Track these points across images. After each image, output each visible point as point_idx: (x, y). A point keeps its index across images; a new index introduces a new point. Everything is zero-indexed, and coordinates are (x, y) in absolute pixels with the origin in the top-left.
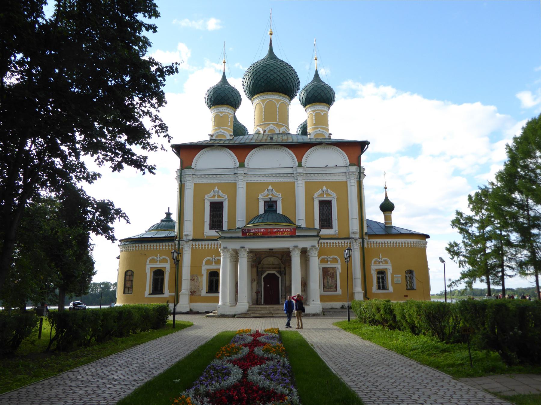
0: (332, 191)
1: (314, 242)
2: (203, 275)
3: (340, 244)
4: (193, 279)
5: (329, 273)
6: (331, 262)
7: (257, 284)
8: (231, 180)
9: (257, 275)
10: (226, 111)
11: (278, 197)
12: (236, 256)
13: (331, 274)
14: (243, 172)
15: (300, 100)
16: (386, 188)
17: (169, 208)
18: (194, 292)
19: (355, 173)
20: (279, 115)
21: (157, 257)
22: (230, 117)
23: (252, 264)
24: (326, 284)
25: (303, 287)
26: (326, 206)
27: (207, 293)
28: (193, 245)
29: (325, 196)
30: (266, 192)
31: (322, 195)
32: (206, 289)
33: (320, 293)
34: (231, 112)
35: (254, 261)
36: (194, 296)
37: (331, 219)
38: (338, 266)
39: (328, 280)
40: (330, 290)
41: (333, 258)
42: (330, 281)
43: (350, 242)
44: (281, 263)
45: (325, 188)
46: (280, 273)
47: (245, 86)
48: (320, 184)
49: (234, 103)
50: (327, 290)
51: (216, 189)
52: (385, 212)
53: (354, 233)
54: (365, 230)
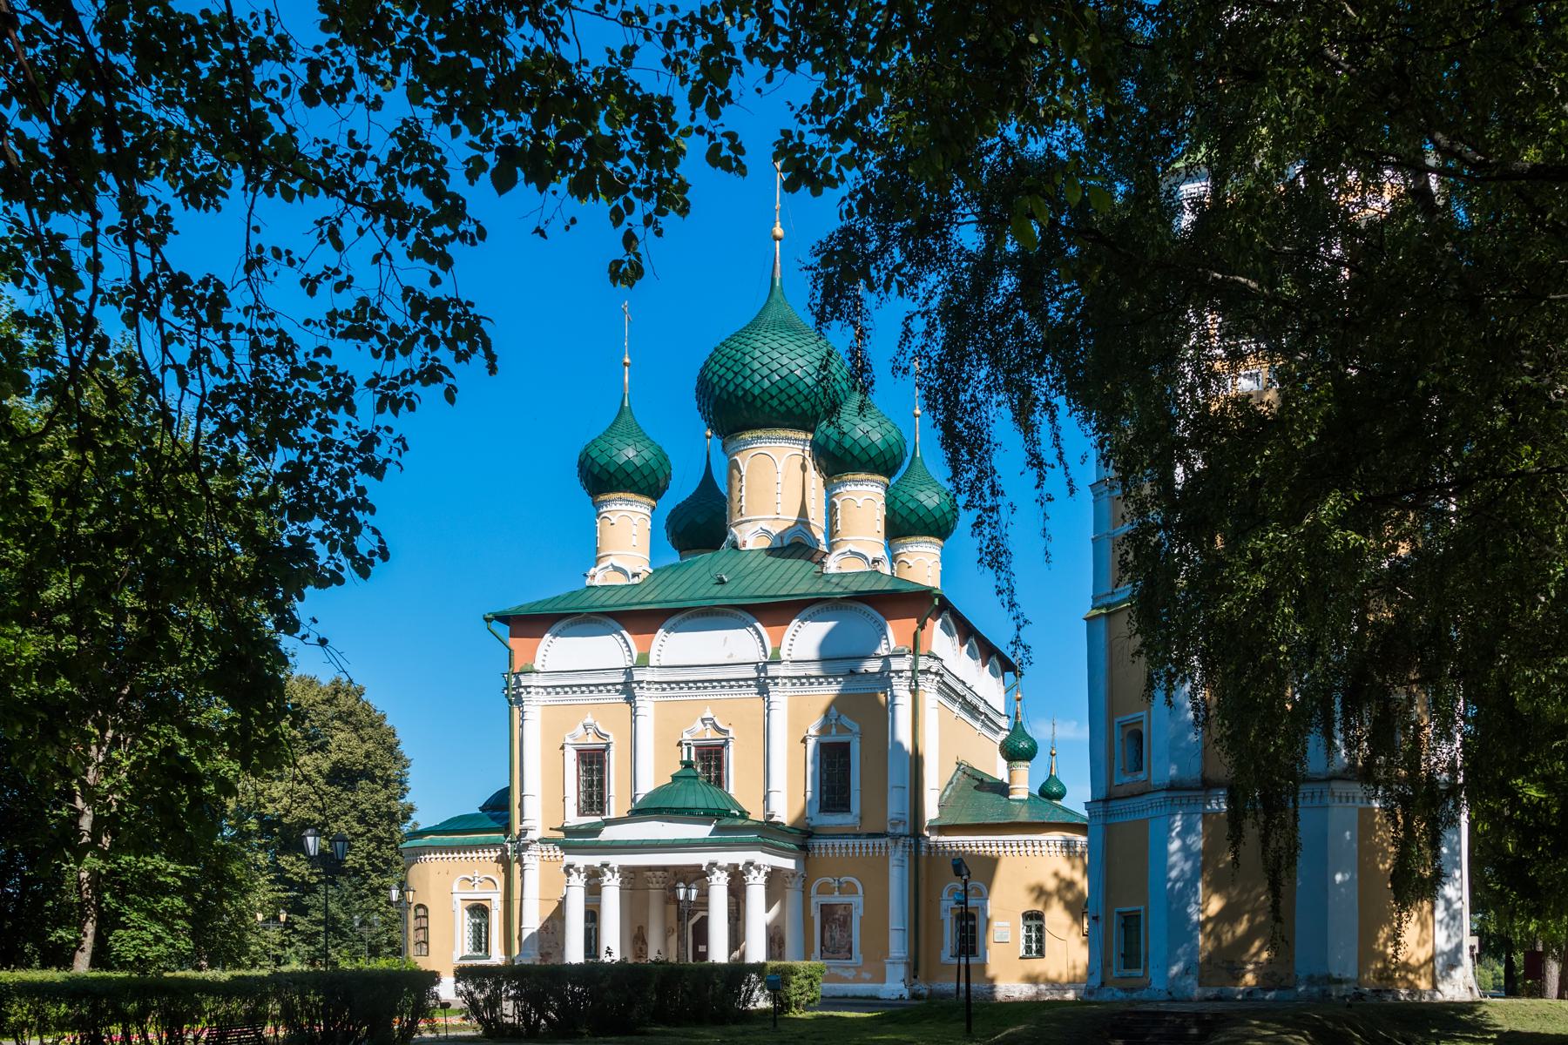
38: (857, 901)
42: (837, 936)
50: (830, 955)
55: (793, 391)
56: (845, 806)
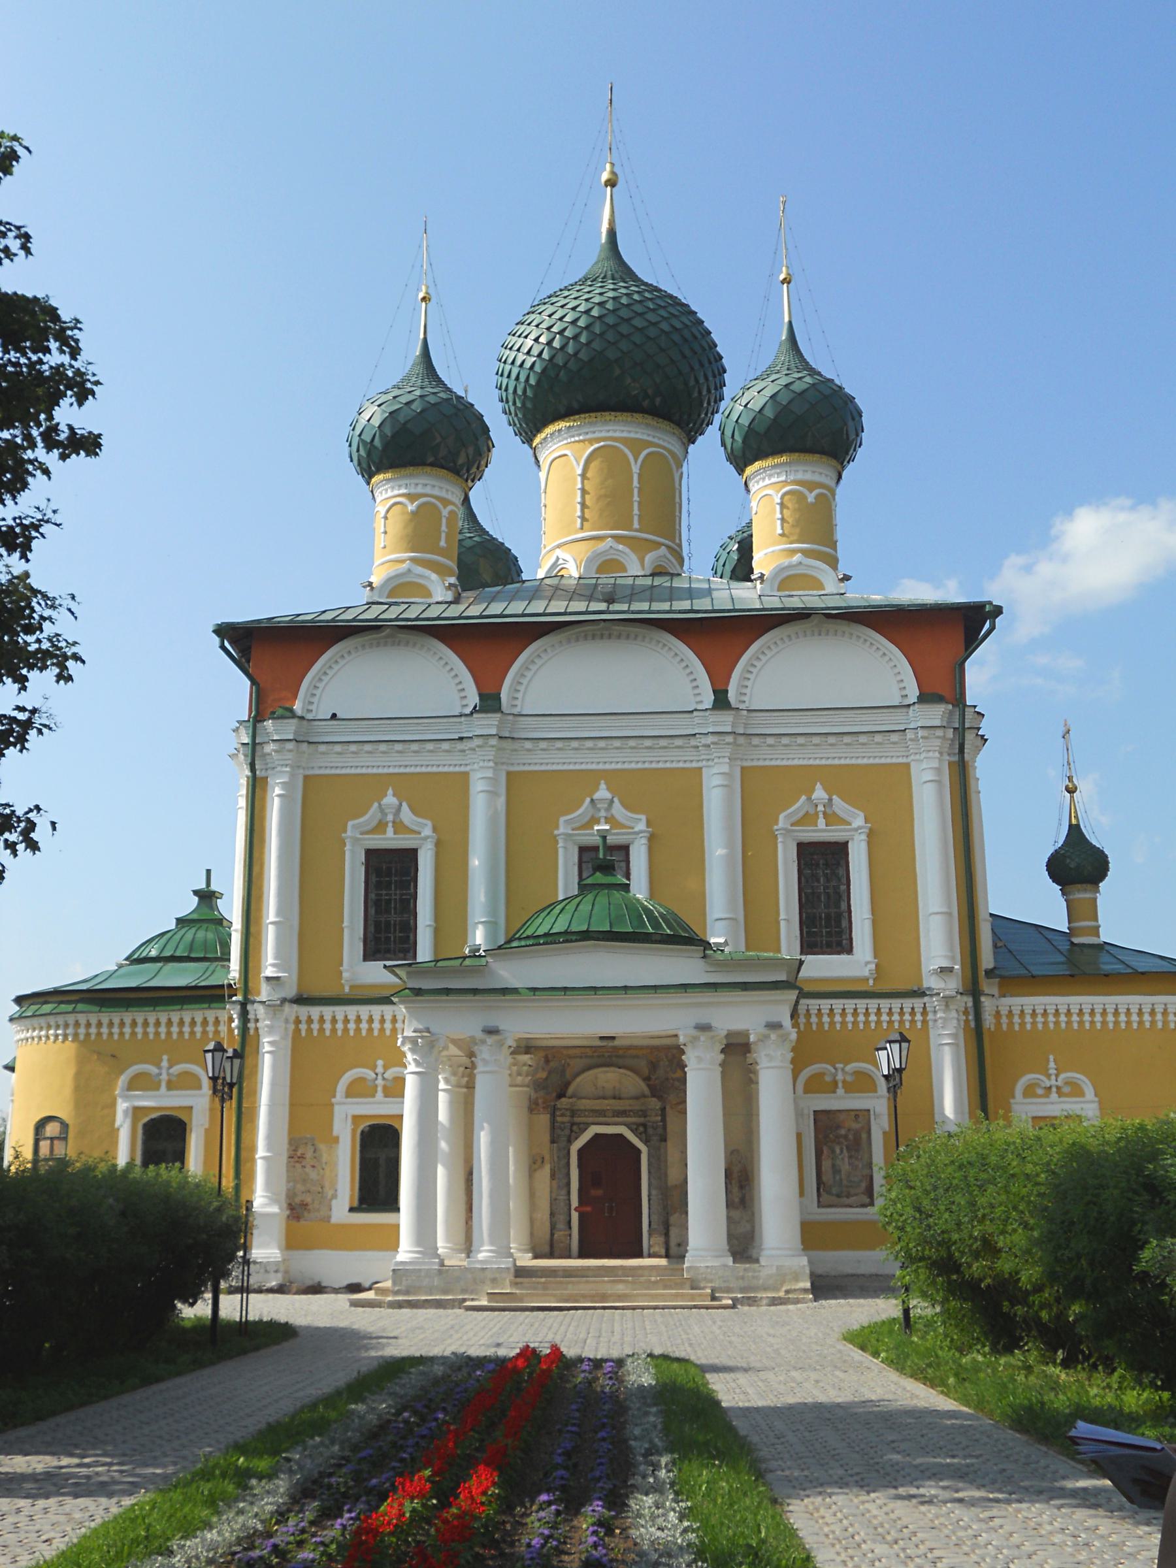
0: (850, 804)
1: (779, 1007)
2: (336, 1140)
3: (885, 1018)
4: (299, 1154)
5: (843, 1132)
6: (849, 1088)
7: (553, 1176)
9: (553, 1142)
12: (465, 1060)
13: (851, 1137)
15: (723, 444)
16: (1071, 791)
17: (208, 872)
18: (304, 1205)
19: (939, 733)
20: (640, 503)
21: (160, 1068)
23: (534, 1096)
24: (827, 1177)
25: (735, 1190)
26: (827, 865)
27: (352, 1210)
28: (298, 1021)
29: (821, 823)
31: (808, 819)
32: (352, 1196)
33: (803, 1209)
34: (449, 497)
35: (538, 1085)
36: (302, 1222)
37: (846, 915)
39: (838, 1162)
40: (845, 1201)
41: (857, 1073)
42: (845, 1167)
43: (925, 1008)
44: (647, 1091)
45: (819, 794)
46: (641, 1130)
47: (506, 390)
52: (1068, 888)
54: (987, 959)
56: (840, 943)
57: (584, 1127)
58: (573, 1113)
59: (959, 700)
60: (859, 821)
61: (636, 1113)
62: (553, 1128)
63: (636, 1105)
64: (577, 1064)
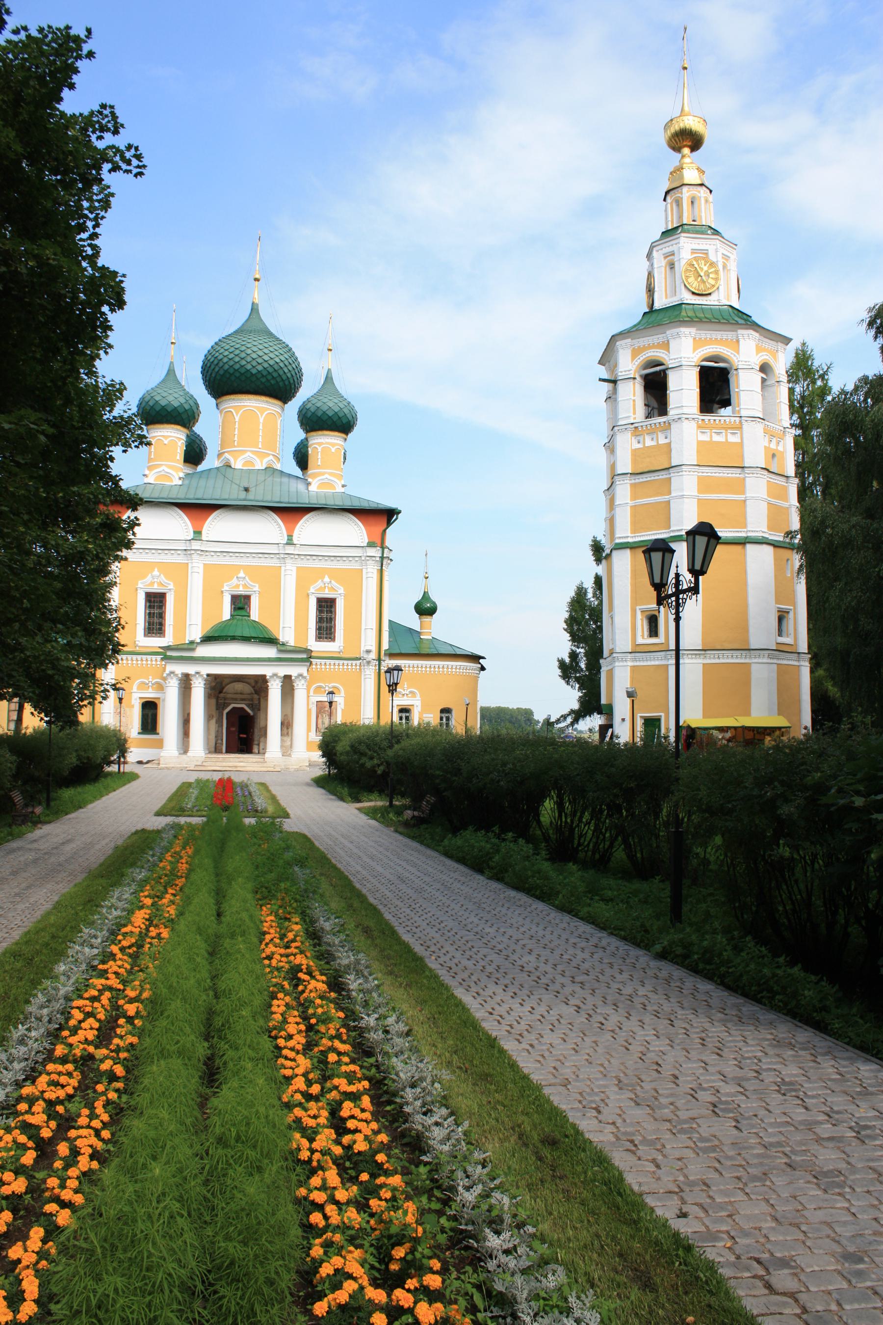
2: (133, 706)
7: (217, 722)
8: (180, 559)
10: (173, 434)
11: (254, 589)
14: (198, 548)
22: (179, 444)
24: (320, 726)
30: (234, 581)
31: (321, 589)
46: (251, 706)
48: (320, 573)
49: (186, 421)
51: (156, 573)
53: (368, 652)
55: (275, 375)
57: (230, 704)
58: (225, 699)
59: (383, 547)
60: (341, 591)
61: (249, 700)
62: (218, 705)
63: (249, 697)
64: (227, 681)
